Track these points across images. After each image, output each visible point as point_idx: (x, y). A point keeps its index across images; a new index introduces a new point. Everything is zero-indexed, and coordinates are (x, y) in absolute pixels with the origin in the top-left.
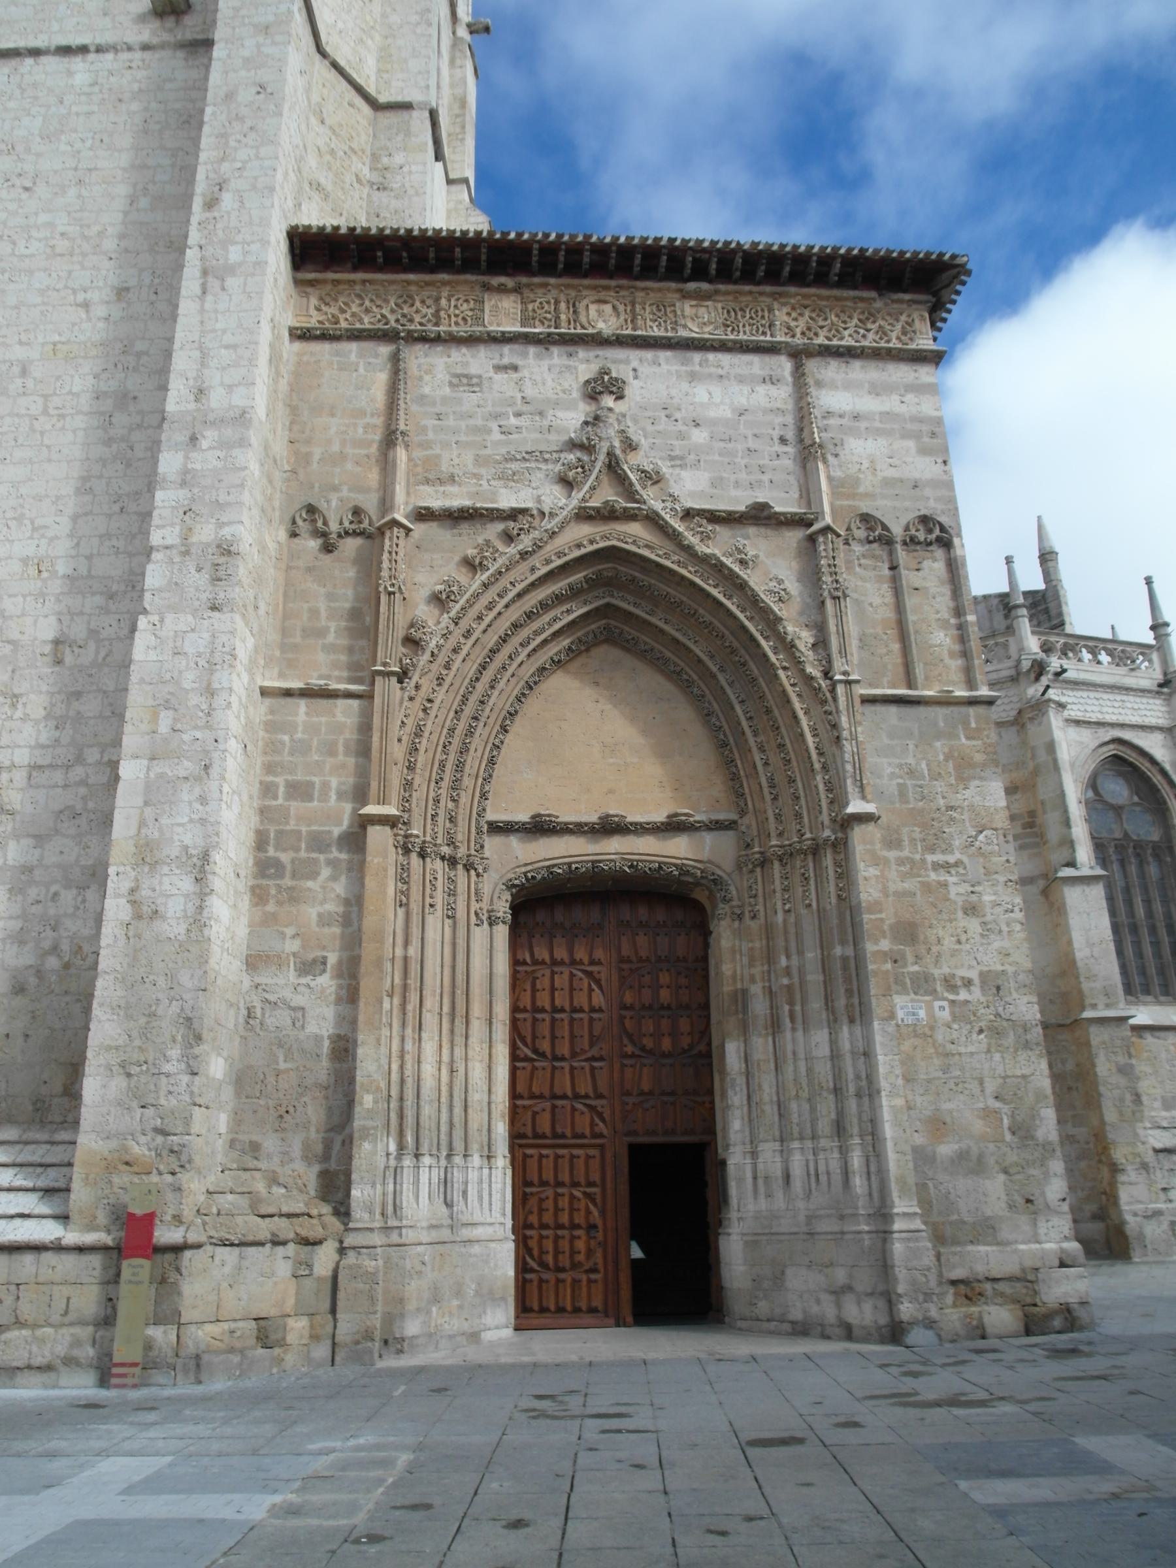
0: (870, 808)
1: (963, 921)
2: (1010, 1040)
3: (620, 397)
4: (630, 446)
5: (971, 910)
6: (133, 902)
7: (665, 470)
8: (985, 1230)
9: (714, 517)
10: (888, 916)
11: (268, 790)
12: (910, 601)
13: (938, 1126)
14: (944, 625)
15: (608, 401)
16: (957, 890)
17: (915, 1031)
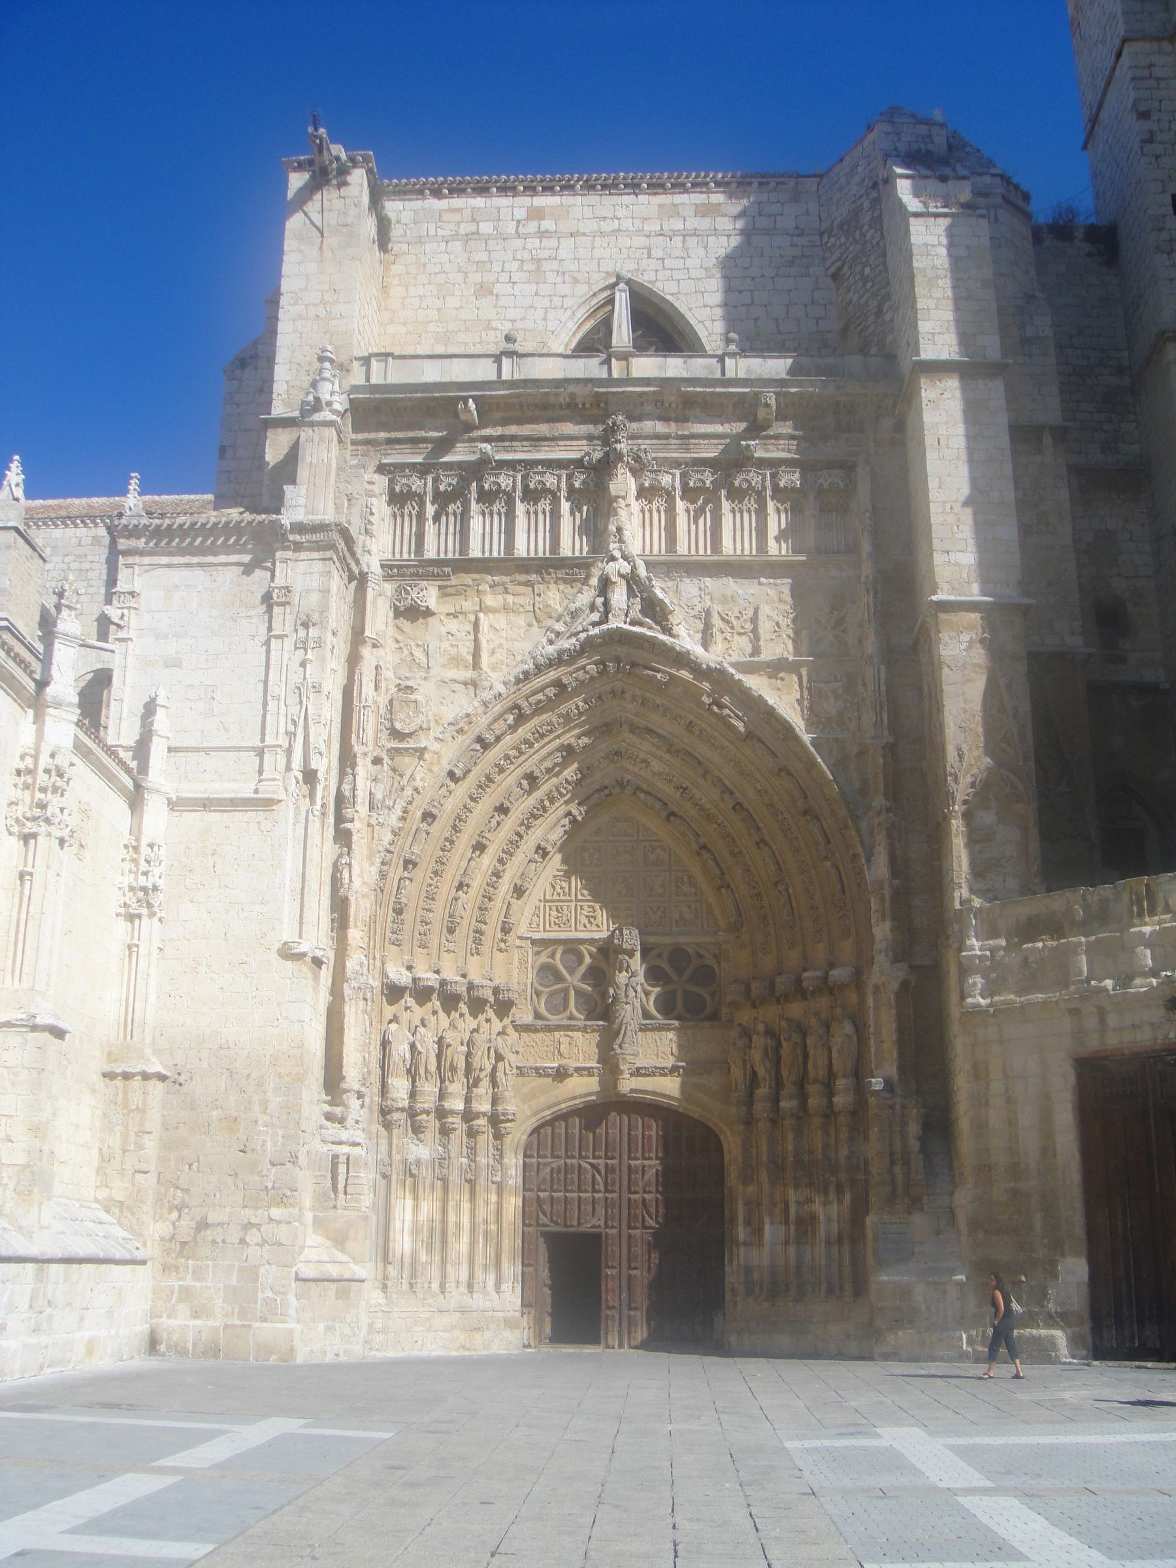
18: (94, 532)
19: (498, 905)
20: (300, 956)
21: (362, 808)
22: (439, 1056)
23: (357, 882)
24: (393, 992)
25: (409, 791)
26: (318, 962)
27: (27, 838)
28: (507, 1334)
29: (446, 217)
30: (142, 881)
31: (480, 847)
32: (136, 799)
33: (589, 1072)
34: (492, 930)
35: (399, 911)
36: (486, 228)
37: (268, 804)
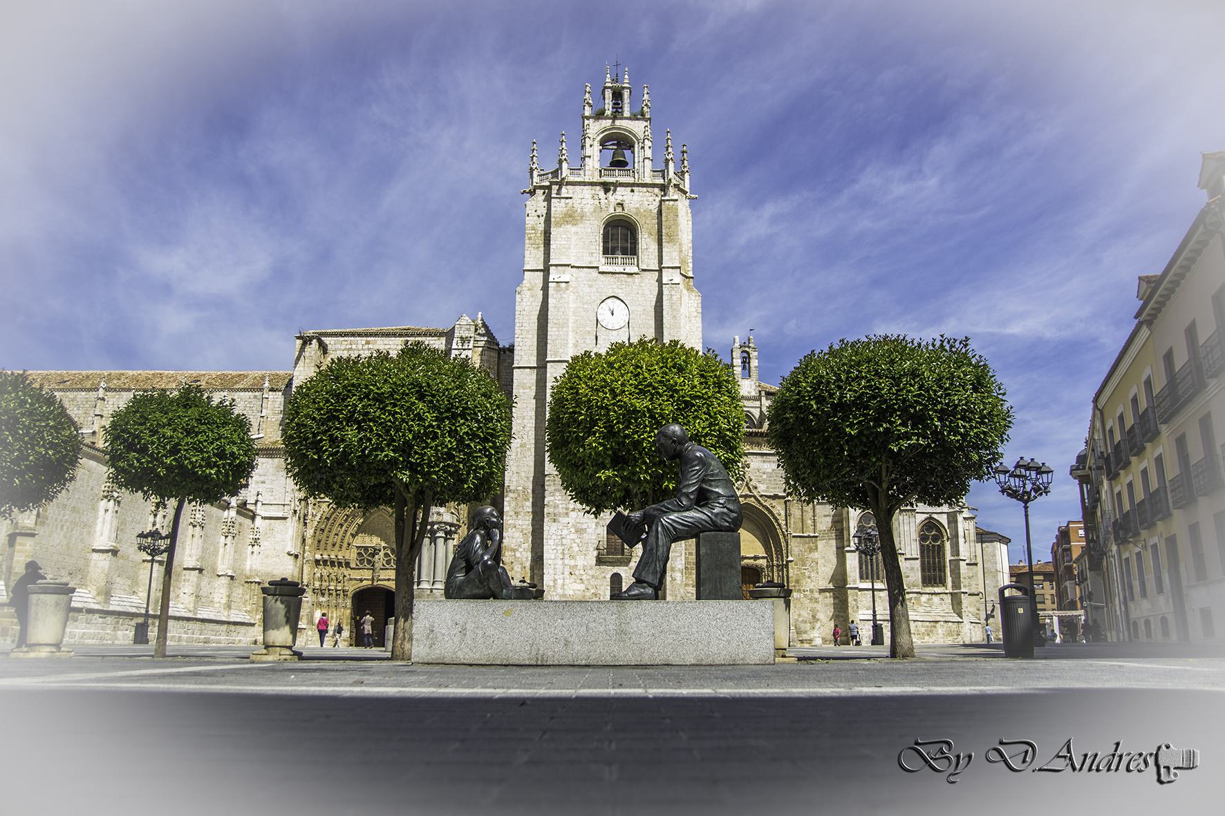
0: (792, 559)
1: (807, 579)
2: (813, 601)
3: (748, 468)
4: (751, 480)
5: (809, 577)
6: (672, 578)
7: (758, 485)
8: (806, 632)
9: (766, 496)
10: (794, 579)
11: (686, 553)
12: (804, 514)
13: (799, 615)
14: (810, 519)
15: (746, 469)
16: (807, 574)
17: (797, 599)
18: (254, 394)
19: (347, 538)
20: (292, 555)
21: (310, 517)
22: (328, 576)
23: (308, 535)
24: (317, 562)
25: (322, 512)
26: (296, 556)
27: (226, 537)
28: (344, 642)
29: (343, 343)
30: (256, 537)
31: (341, 525)
32: (253, 518)
33: (368, 580)
34: (345, 545)
35: (319, 541)
36: (354, 347)
37: (285, 518)
